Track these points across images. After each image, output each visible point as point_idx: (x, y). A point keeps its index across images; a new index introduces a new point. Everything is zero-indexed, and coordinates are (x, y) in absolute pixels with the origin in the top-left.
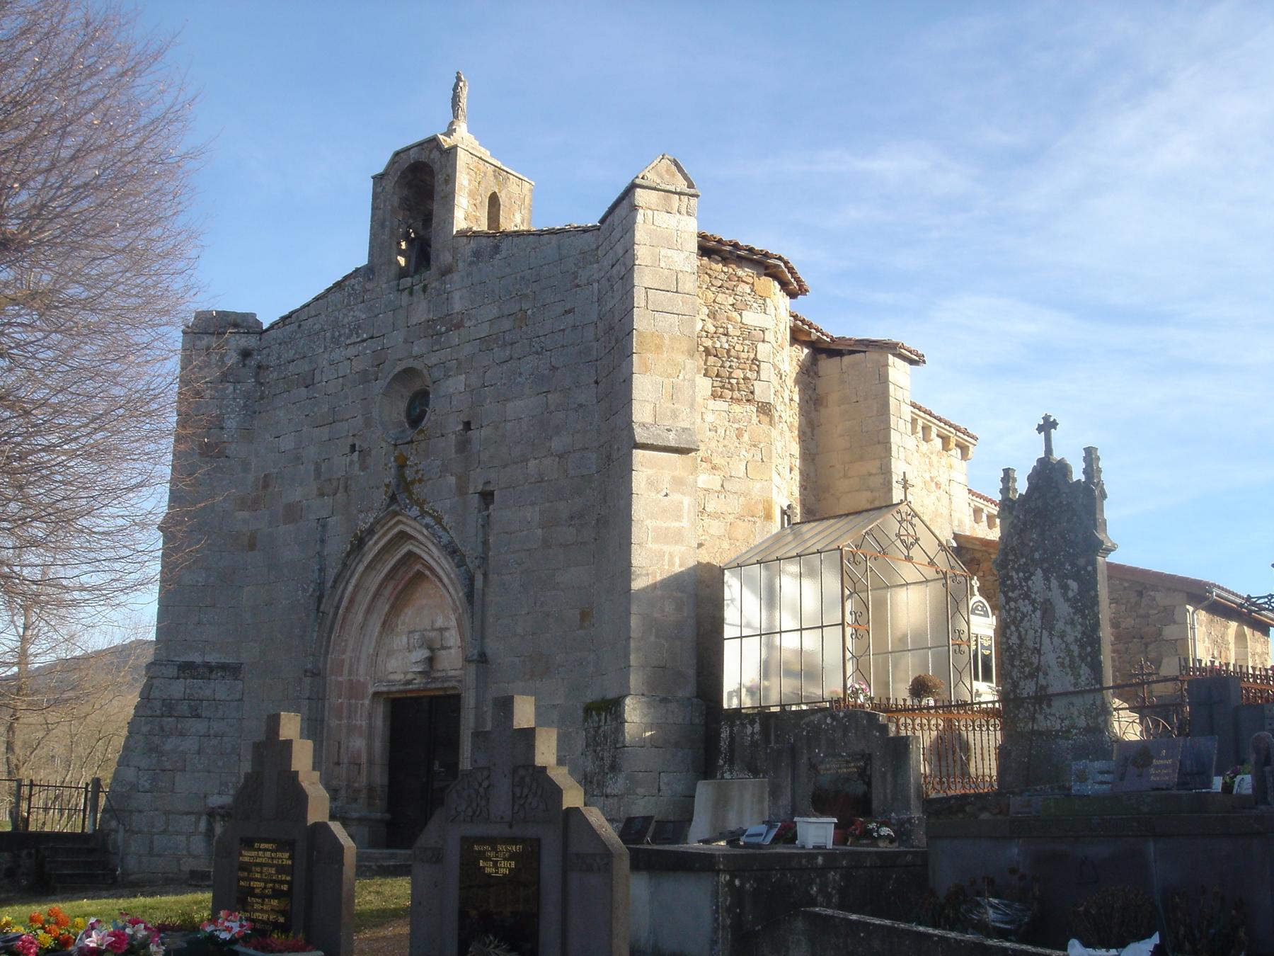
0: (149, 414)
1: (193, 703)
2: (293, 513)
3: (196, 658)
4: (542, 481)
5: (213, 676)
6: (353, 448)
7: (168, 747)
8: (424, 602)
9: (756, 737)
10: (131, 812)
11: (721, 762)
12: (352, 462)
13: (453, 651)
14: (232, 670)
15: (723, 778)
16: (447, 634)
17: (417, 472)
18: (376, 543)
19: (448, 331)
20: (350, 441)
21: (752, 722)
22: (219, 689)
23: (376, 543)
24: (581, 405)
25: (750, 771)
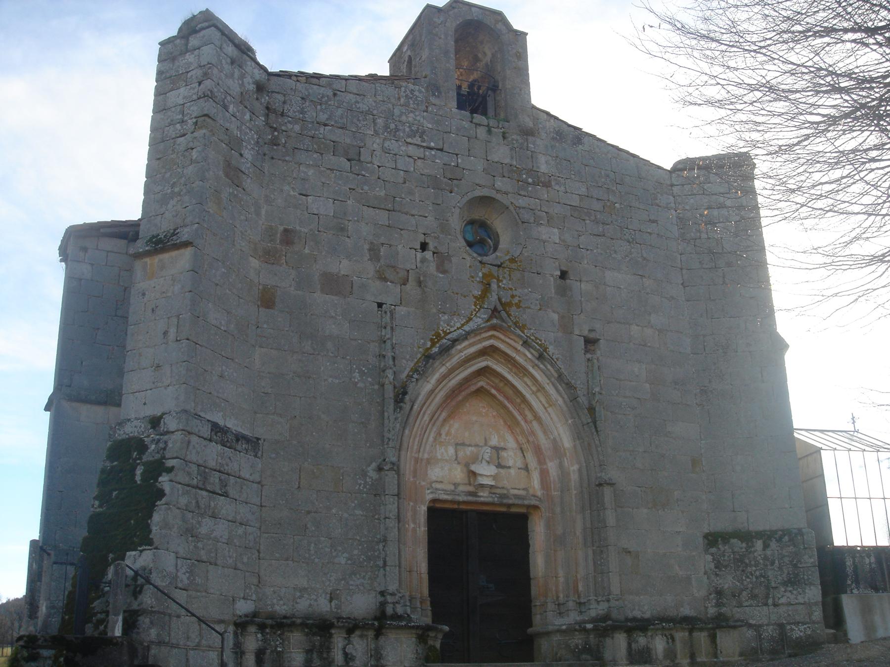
0: (211, 92)
1: (223, 477)
2: (334, 284)
3: (232, 424)
4: (645, 345)
5: (239, 447)
6: (424, 247)
7: (203, 530)
8: (474, 418)
9: (873, 566)
10: (170, 615)
11: (849, 582)
12: (423, 261)
13: (512, 471)
14: (253, 444)
15: (852, 593)
16: (504, 454)
17: (513, 296)
18: (465, 348)
19: (534, 184)
20: (421, 238)
21: (869, 556)
22: (242, 463)
23: (465, 348)
24: (672, 298)
25: (872, 588)
